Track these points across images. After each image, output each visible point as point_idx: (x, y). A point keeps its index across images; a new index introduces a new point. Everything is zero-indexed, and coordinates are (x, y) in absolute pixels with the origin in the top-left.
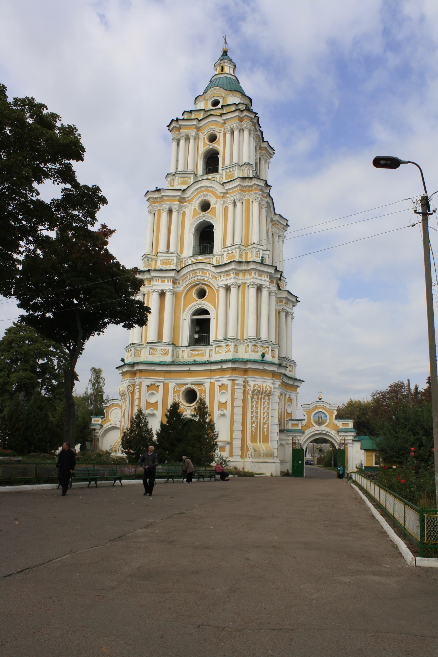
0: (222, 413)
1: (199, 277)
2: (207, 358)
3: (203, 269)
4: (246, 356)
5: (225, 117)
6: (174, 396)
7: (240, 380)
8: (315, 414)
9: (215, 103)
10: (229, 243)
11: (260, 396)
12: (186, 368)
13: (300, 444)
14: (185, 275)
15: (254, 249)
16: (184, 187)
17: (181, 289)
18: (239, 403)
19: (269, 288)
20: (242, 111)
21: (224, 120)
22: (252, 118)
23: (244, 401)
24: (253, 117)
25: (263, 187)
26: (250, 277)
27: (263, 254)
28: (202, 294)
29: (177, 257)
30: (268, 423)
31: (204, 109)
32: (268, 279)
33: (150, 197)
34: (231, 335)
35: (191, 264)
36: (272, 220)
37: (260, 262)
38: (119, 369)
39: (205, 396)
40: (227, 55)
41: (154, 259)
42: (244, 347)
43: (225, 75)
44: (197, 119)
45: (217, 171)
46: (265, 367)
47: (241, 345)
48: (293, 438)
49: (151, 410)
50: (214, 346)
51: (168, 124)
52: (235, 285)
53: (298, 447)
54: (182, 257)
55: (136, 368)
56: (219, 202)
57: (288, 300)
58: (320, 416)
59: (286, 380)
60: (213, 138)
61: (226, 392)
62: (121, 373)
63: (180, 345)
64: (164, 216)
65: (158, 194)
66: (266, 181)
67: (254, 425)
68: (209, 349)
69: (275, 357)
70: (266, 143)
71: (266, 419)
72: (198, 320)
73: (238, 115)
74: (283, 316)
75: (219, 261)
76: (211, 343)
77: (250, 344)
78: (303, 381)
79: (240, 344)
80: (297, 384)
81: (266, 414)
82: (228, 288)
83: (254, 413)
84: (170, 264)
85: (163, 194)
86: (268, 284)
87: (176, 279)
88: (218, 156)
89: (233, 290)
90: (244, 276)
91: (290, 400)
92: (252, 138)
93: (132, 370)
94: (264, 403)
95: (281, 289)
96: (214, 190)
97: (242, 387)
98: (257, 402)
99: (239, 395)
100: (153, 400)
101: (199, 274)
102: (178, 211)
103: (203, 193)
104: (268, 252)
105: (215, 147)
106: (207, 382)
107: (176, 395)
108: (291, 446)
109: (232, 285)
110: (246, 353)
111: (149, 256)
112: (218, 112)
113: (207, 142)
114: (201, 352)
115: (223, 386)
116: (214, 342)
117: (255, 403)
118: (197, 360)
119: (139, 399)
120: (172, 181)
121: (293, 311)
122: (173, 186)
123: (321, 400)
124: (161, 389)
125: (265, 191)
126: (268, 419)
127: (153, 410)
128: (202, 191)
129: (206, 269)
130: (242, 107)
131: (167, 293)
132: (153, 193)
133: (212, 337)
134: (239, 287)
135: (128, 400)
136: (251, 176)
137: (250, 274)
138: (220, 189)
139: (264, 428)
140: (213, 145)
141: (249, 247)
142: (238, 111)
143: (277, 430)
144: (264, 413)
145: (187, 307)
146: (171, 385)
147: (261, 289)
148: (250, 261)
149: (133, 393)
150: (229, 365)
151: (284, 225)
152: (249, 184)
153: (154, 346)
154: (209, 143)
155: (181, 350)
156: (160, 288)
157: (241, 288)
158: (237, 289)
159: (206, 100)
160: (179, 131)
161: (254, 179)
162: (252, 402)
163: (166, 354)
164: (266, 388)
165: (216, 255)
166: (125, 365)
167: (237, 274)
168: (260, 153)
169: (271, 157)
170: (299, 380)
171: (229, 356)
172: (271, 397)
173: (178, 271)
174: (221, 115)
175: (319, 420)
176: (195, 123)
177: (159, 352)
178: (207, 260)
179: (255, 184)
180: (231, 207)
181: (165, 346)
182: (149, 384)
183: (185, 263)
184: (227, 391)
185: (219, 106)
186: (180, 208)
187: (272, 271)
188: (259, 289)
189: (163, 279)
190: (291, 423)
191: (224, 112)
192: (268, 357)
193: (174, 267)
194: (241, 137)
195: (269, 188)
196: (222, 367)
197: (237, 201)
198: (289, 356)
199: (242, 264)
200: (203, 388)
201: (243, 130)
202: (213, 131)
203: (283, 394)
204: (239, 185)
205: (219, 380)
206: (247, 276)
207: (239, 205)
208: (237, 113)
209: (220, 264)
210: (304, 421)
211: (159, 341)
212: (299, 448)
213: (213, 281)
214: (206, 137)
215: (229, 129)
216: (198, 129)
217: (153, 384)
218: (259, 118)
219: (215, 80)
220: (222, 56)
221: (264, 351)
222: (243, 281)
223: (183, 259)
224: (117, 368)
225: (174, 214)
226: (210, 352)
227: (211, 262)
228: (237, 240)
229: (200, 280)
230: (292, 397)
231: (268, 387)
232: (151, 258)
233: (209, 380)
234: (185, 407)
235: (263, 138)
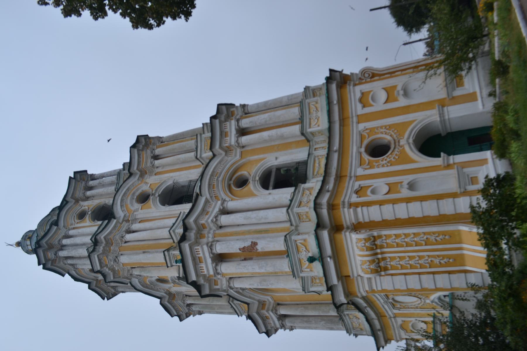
0: (402, 92)
1: (220, 179)
3: (212, 175)
6: (378, 167)
14: (211, 197)
39: (378, 127)
61: (372, 93)
101: (216, 180)
105: (93, 208)
106: (357, 127)
107: (377, 164)
109: (238, 123)
115: (363, 100)
131: (225, 205)
146: (360, 172)
177: (305, 199)
181: (299, 192)
182: (354, 196)
200: (367, 133)
202: (76, 214)
214: (76, 221)
217: (357, 192)
234: (396, 150)
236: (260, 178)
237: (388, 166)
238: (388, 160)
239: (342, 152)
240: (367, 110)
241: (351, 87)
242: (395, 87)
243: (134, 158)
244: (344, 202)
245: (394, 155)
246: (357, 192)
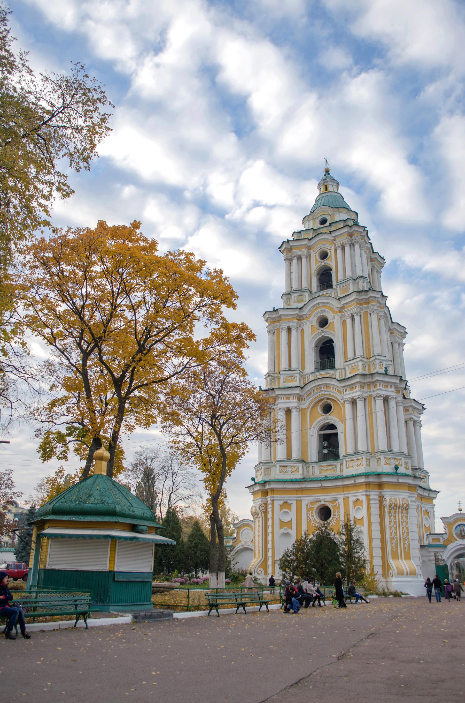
1: (323, 393)
2: (338, 473)
3: (327, 384)
4: (380, 470)
5: (334, 234)
6: (307, 514)
7: (374, 494)
8: (456, 527)
9: (323, 222)
10: (350, 355)
11: (397, 510)
12: (318, 485)
13: (444, 560)
14: (309, 391)
15: (376, 361)
16: (300, 305)
17: (306, 405)
18: (375, 519)
19: (396, 398)
20: (351, 227)
21: (333, 237)
22: (361, 232)
23: (381, 516)
24: (362, 231)
25: (379, 298)
26: (376, 389)
27: (386, 365)
28: (327, 409)
29: (299, 373)
30: (409, 538)
31: (313, 229)
32: (393, 390)
33: (268, 318)
34: (361, 448)
35: (314, 380)
36: (390, 330)
37: (384, 373)
38: (250, 488)
40: (329, 174)
41: (277, 377)
42: (376, 460)
43: (330, 194)
44: (307, 238)
45: (331, 286)
46: (400, 480)
47: (373, 458)
48: (435, 554)
49: (285, 529)
50: (344, 461)
51: (280, 246)
52: (360, 398)
53: (441, 564)
54: (304, 374)
55: (267, 487)
56: (336, 317)
57: (415, 408)
58: (462, 529)
59: (420, 492)
60: (324, 256)
62: (252, 493)
63: (309, 461)
64: (284, 334)
65: (276, 314)
66: (382, 292)
67: (394, 542)
68: (339, 464)
69: (408, 469)
70: (377, 254)
71: (405, 534)
72: (324, 435)
73: (347, 231)
74: (411, 425)
75: (342, 375)
76: (341, 458)
77: (382, 457)
78: (439, 492)
79: (372, 457)
80: (432, 495)
81: (405, 529)
82: (354, 402)
83: (393, 528)
84: (293, 380)
85: (280, 313)
86: (394, 394)
87: (300, 396)
88: (331, 272)
89: (360, 404)
90: (369, 388)
91: (427, 513)
92: (363, 252)
93: (263, 489)
94: (402, 517)
95: (406, 397)
96: (331, 306)
97: (378, 502)
98: (395, 517)
99: (375, 510)
100: (286, 519)
102: (297, 329)
103: (320, 310)
104: (390, 363)
106: (340, 498)
107: (310, 513)
108: (434, 562)
110: (378, 466)
111: (272, 375)
112: (327, 230)
113: (319, 260)
114: (331, 467)
115: (357, 501)
116: (344, 456)
117: (392, 518)
118: (328, 476)
119: (273, 518)
120: (288, 300)
121: (421, 419)
122: (289, 305)
123: (461, 512)
124: (294, 507)
125: (381, 302)
126: (408, 534)
127: (286, 529)
128: (319, 308)
129: (330, 384)
130: (350, 223)
131: (293, 410)
132: (270, 313)
133: (342, 452)
134: (365, 399)
135: (261, 519)
136: (366, 289)
137: (375, 386)
138: (336, 304)
139: (404, 544)
140: (325, 262)
141: (372, 359)
142: (347, 227)
143: (419, 547)
144: (403, 528)
145: (314, 422)
146: (304, 503)
147: (387, 400)
148: (375, 373)
149: (266, 513)
150: (363, 480)
151: (402, 333)
152: (366, 297)
153: (283, 464)
154: (321, 260)
155: (311, 467)
156: (285, 406)
157: (367, 401)
158: (363, 402)
159: (314, 219)
160: (290, 252)
161: (370, 291)
162: (390, 517)
163: (297, 470)
164: (403, 501)
165: (338, 369)
166: (256, 483)
167: (362, 387)
168: (371, 264)
169: (382, 267)
170: (434, 491)
171: (362, 470)
172: (408, 511)
173: (302, 388)
174: (330, 232)
175: (461, 533)
176: (306, 242)
177: (289, 469)
178: (330, 375)
179: (371, 296)
180: (349, 321)
182: (281, 502)
183: (308, 379)
184: (362, 506)
185: (328, 224)
186: (299, 325)
187: (397, 381)
188: (386, 400)
189: (288, 397)
190: (431, 537)
191: (333, 230)
192: (402, 470)
193: (297, 384)
194: (352, 251)
195: (386, 298)
196: (355, 481)
197: (355, 315)
198: (421, 467)
199: (366, 377)
201: (354, 245)
203: (420, 507)
204: (356, 298)
205: (353, 496)
206: (372, 389)
207: (357, 318)
208: (346, 229)
209: (343, 378)
210: (445, 535)
211: (289, 458)
212: (443, 564)
213: (337, 395)
214: (317, 254)
215: (340, 245)
216: (309, 248)
217: (286, 503)
218: (367, 231)
219: (321, 199)
220: (325, 175)
221: (397, 463)
222: (369, 394)
223: (305, 375)
224: (247, 487)
225: (294, 332)
226: (340, 466)
227: (334, 377)
228: (359, 353)
229: (325, 395)
230: (429, 510)
231: (405, 500)
232: (274, 377)
233: (343, 496)
235: (372, 249)
236: (327, 423)
237: (307, 520)
238: (312, 520)
239: (322, 489)
240: (351, 505)
241: (364, 493)
242: (363, 525)
243: (350, 298)
244: (273, 497)
245: (315, 524)
246: (286, 503)
